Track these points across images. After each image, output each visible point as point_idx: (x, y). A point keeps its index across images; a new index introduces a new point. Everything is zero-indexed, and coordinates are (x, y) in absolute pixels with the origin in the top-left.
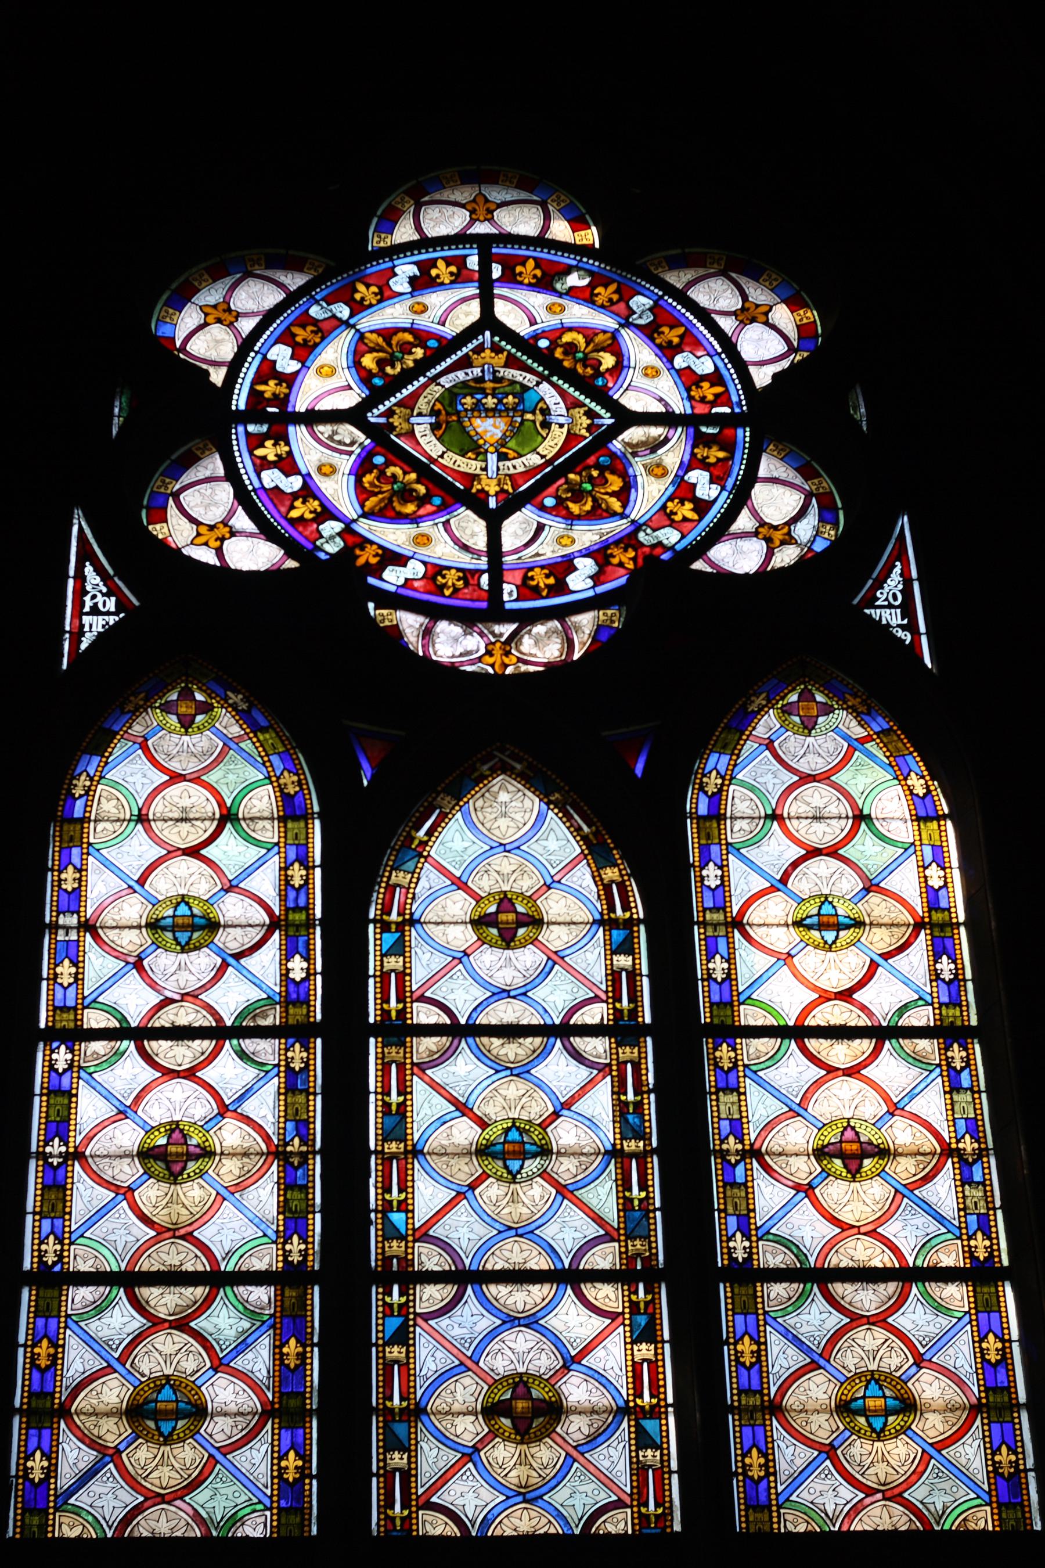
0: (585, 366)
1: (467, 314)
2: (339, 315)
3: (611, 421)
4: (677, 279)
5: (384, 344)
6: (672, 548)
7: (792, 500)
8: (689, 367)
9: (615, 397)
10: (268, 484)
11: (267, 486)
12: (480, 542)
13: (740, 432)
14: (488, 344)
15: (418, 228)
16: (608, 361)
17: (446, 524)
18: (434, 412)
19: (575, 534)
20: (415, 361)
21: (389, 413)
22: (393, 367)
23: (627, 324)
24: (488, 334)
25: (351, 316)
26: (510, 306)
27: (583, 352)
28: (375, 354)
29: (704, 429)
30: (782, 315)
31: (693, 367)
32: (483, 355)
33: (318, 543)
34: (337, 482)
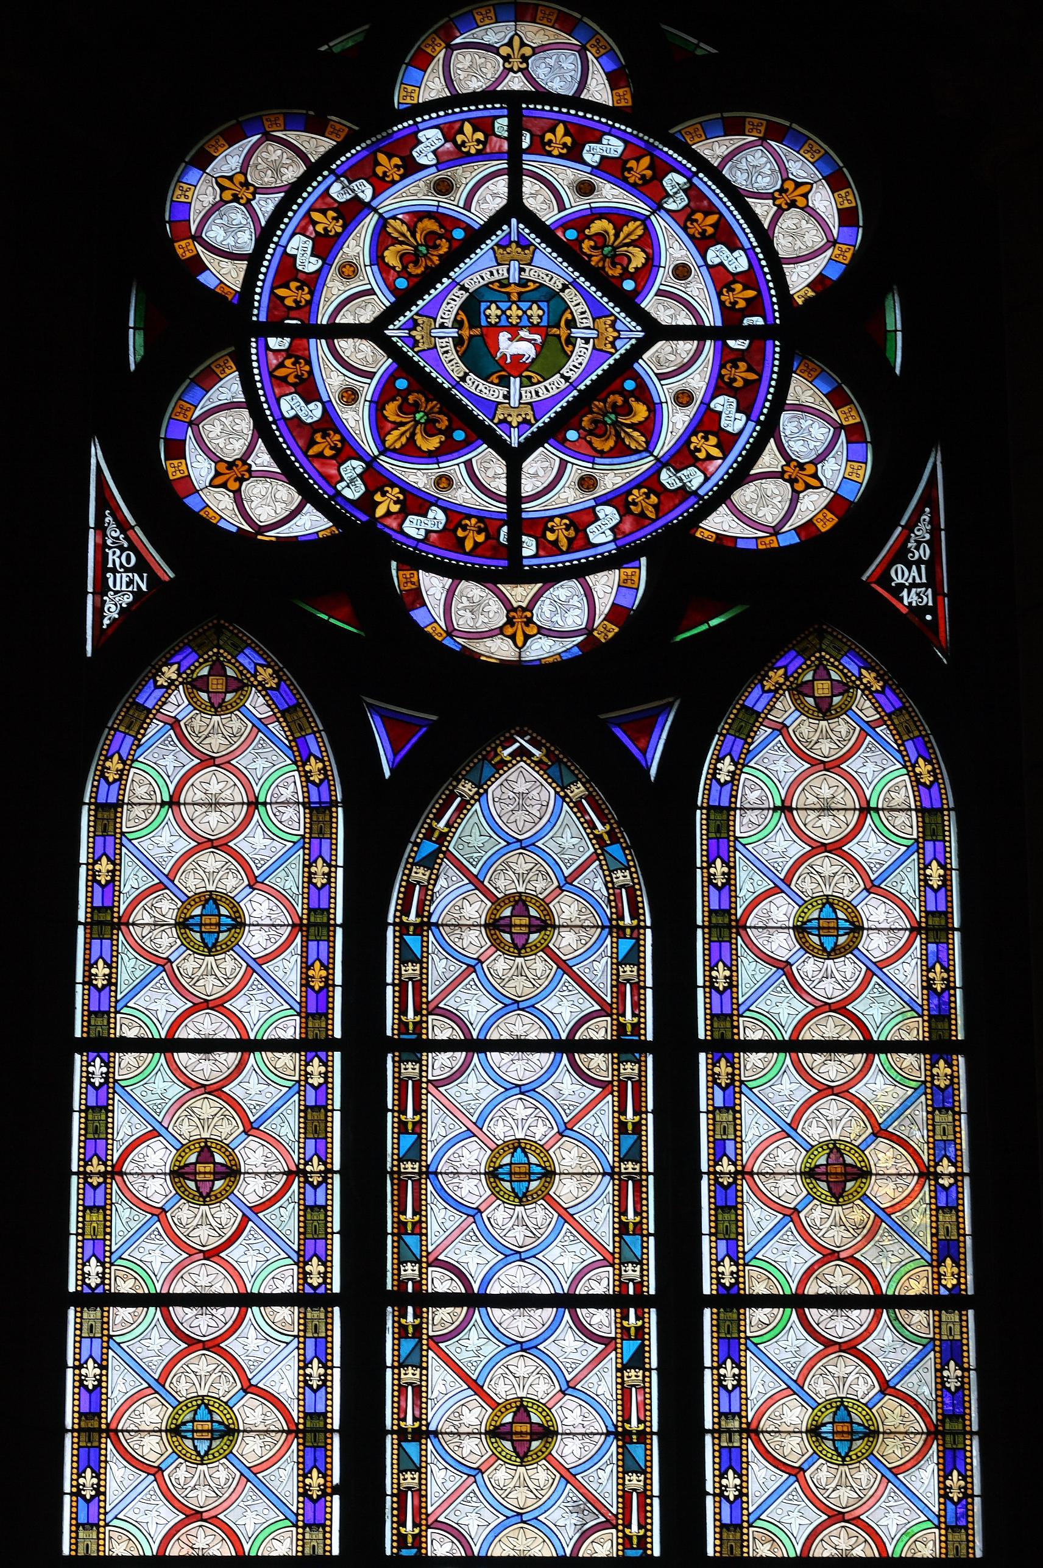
0: (614, 265)
1: (495, 195)
2: (361, 195)
3: (641, 335)
4: (713, 150)
5: (408, 234)
6: (695, 493)
7: (821, 432)
8: (721, 264)
9: (643, 305)
10: (288, 413)
11: (287, 415)
12: (500, 486)
13: (769, 343)
14: (514, 237)
15: (449, 81)
16: (638, 259)
17: (468, 464)
18: (458, 324)
19: (597, 474)
20: (440, 256)
21: (413, 324)
22: (416, 264)
23: (658, 208)
24: (514, 221)
25: (374, 197)
26: (538, 186)
27: (612, 246)
28: (399, 247)
29: (732, 343)
30: (823, 200)
31: (726, 263)
32: (508, 250)
33: (339, 487)
34: (357, 412)
